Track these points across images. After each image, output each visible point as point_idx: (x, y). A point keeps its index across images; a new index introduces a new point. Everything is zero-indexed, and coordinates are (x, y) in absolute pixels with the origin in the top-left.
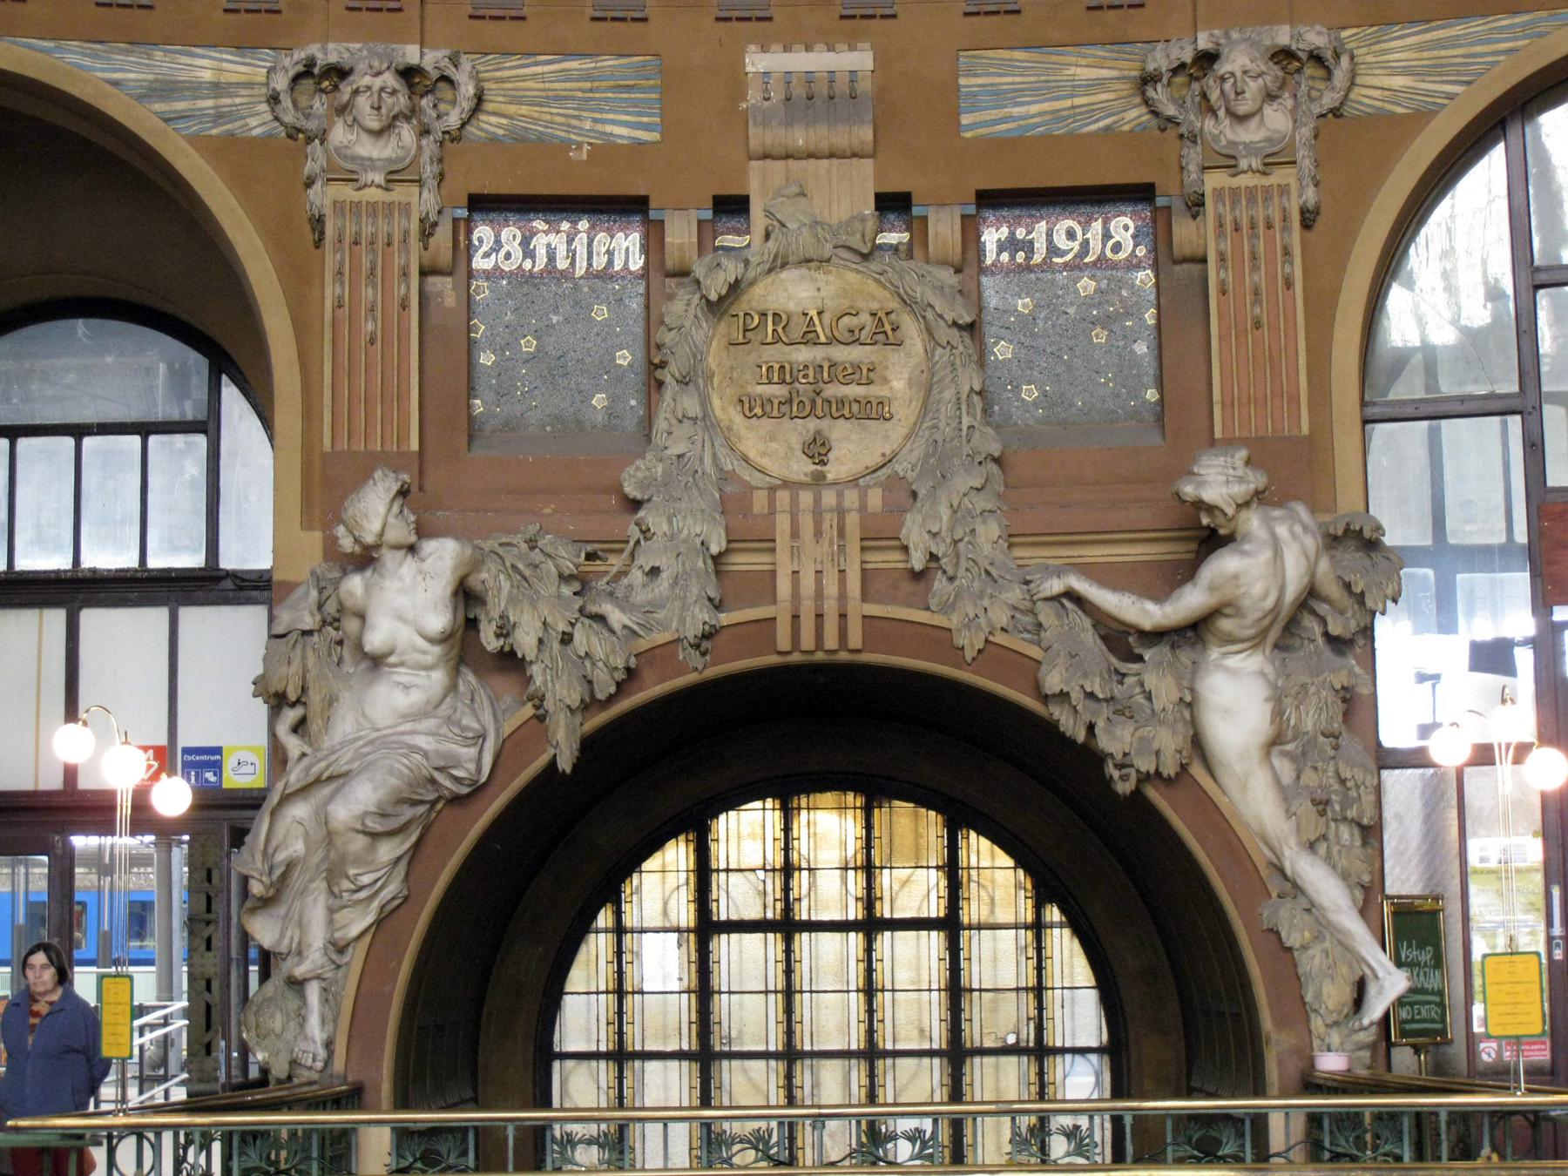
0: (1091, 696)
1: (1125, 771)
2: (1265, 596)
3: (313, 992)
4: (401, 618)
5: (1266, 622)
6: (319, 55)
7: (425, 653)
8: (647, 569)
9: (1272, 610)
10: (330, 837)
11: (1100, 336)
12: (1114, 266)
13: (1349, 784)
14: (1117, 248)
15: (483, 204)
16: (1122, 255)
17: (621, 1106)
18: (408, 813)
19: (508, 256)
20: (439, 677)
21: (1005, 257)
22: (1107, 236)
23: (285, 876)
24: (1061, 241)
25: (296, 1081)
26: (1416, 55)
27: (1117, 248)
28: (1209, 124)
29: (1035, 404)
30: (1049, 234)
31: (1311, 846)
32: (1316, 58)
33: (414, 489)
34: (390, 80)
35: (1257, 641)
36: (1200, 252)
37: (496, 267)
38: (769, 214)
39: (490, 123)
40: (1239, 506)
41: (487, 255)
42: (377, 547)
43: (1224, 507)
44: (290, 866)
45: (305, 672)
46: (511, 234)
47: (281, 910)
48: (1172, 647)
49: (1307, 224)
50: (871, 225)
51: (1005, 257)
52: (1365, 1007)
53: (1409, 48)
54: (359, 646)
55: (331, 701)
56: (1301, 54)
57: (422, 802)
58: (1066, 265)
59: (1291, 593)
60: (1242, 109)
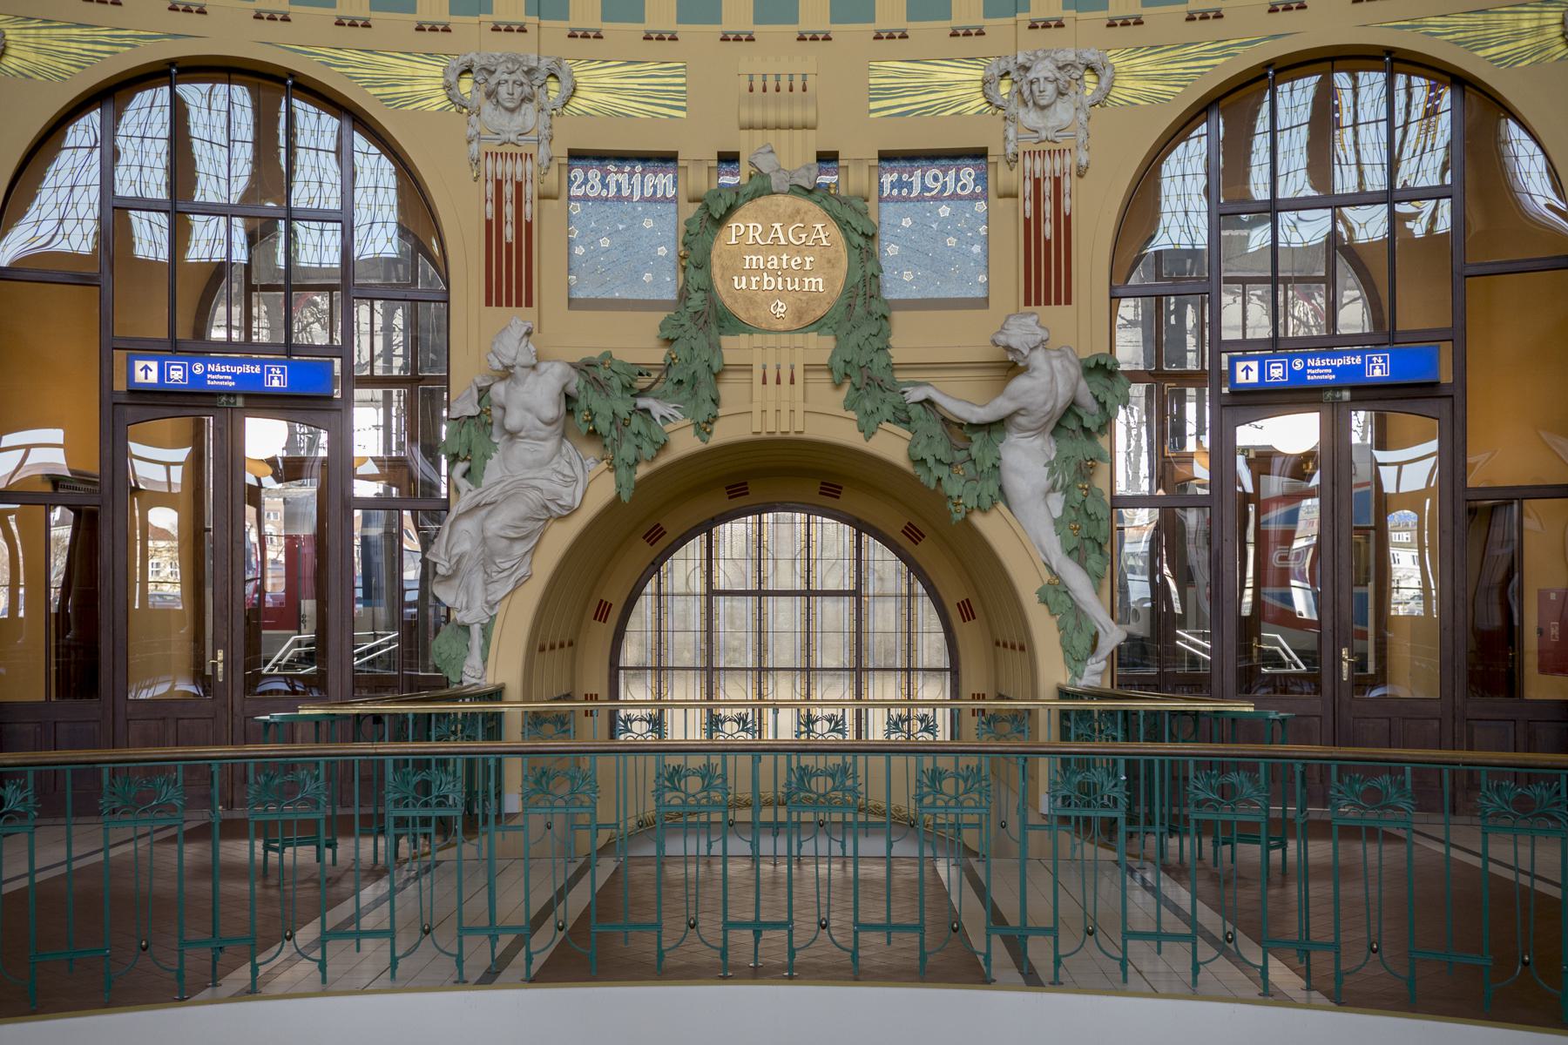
0: (939, 461)
1: (958, 507)
2: (1045, 404)
3: (476, 631)
4: (529, 410)
5: (1045, 419)
6: (476, 59)
7: (541, 430)
8: (675, 380)
9: (1048, 413)
10: (484, 540)
11: (951, 241)
12: (961, 198)
13: (1093, 517)
14: (964, 187)
15: (576, 156)
16: (966, 192)
17: (660, 700)
18: (531, 525)
19: (592, 187)
20: (550, 445)
21: (895, 192)
22: (958, 179)
23: (458, 562)
24: (929, 182)
25: (465, 684)
26: (1154, 68)
27: (964, 187)
28: (1022, 112)
29: (911, 283)
30: (923, 177)
31: (1069, 553)
32: (1090, 68)
33: (535, 331)
34: (519, 76)
35: (1038, 431)
36: (1014, 191)
37: (585, 195)
38: (752, 164)
39: (578, 104)
40: (1031, 349)
41: (579, 187)
42: (513, 367)
43: (1021, 349)
44: (461, 557)
45: (470, 442)
46: (594, 175)
47: (456, 582)
48: (989, 432)
49: (1080, 176)
50: (815, 171)
51: (895, 192)
52: (1098, 649)
53: (1149, 63)
54: (502, 426)
55: (486, 457)
56: (1080, 66)
57: (540, 520)
58: (933, 198)
59: (1061, 403)
60: (1043, 102)
